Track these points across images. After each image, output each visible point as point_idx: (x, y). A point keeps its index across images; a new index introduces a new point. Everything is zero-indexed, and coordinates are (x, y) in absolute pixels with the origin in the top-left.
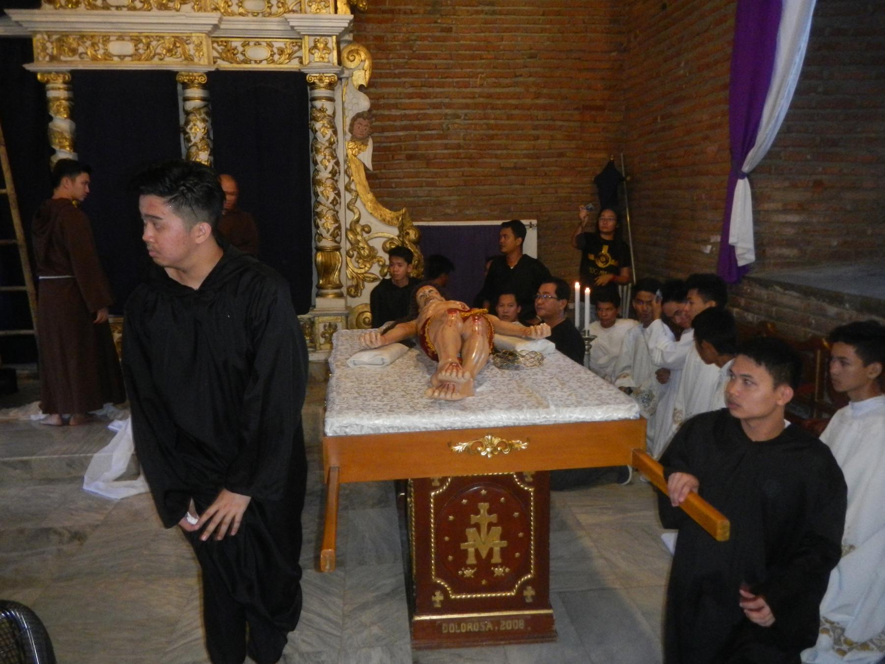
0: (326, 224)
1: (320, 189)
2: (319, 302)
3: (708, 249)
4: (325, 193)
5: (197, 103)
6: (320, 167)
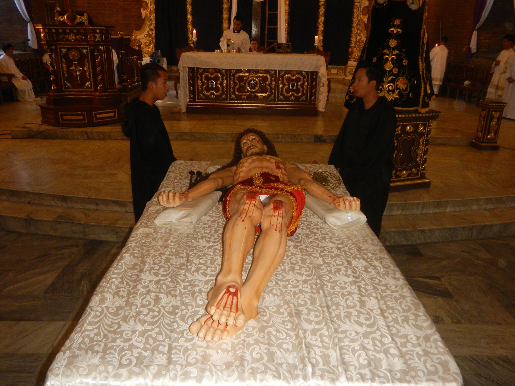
0: (353, 39)
1: (353, 29)
2: (349, 63)
3: (464, 49)
4: (354, 30)
5: (323, 3)
6: (354, 22)
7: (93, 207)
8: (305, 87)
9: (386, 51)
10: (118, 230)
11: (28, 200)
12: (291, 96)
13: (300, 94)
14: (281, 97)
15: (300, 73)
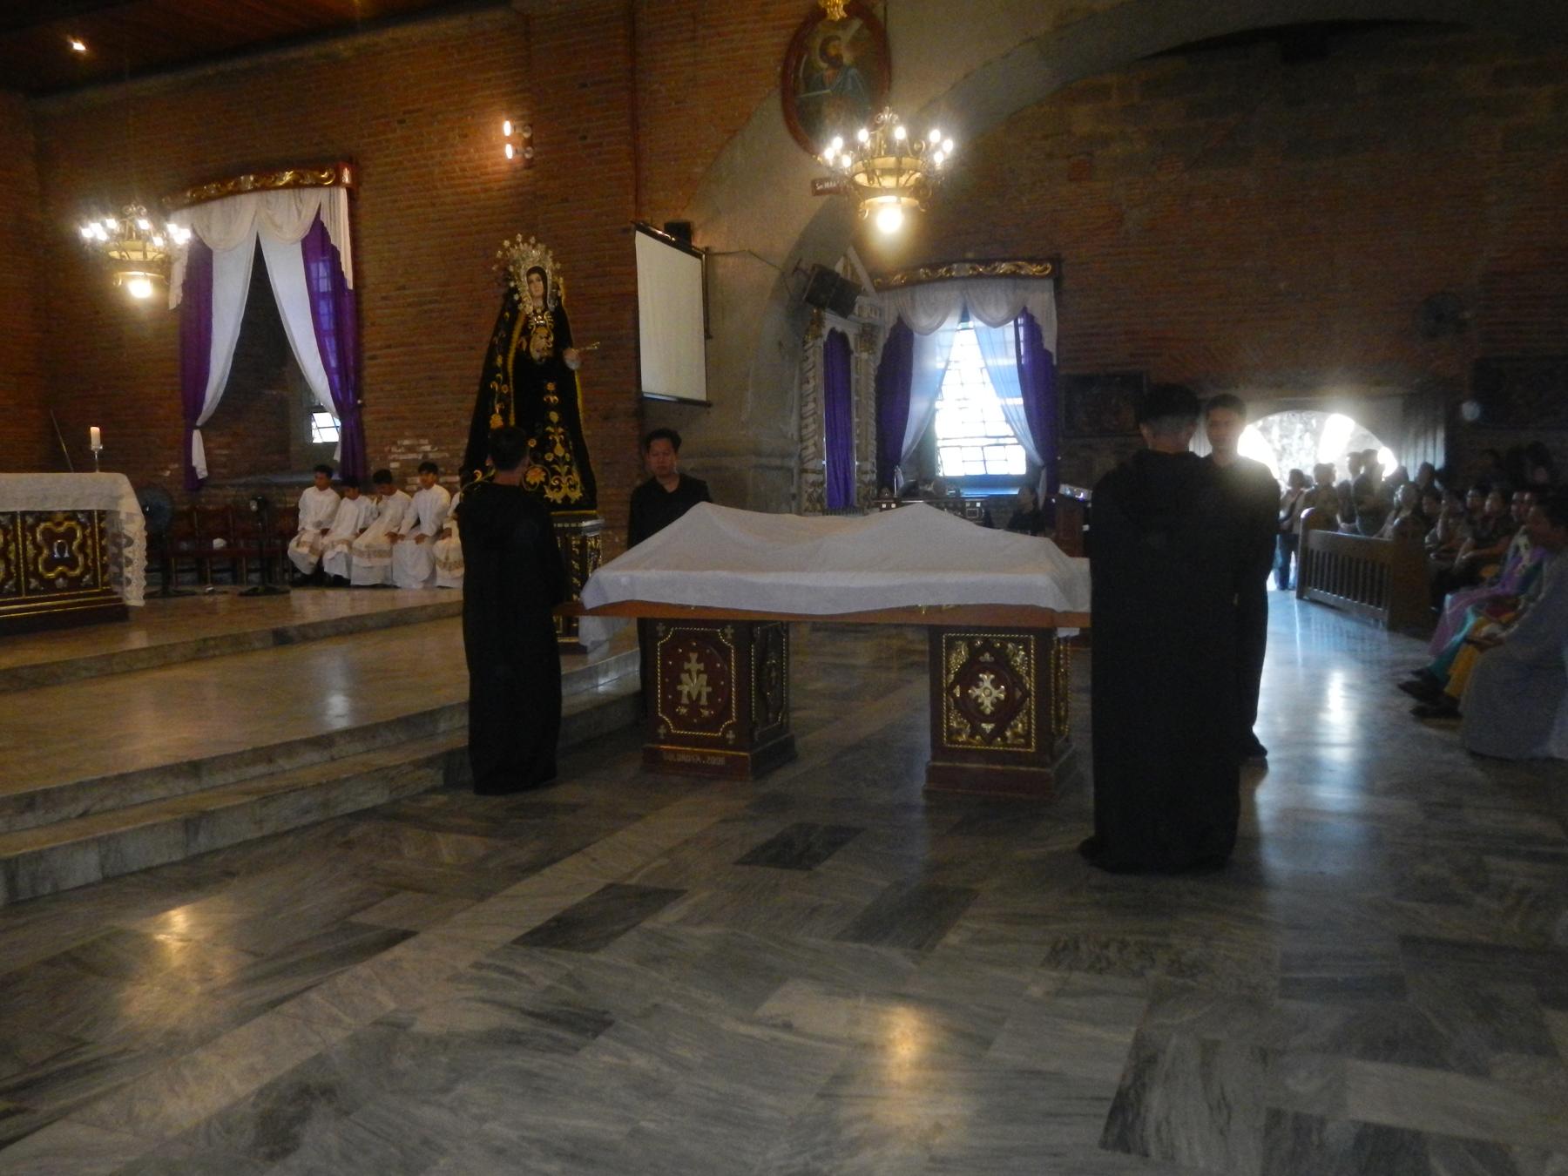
3: (168, 473)
7: (261, 769)
8: (89, 551)
9: (549, 429)
10: (393, 773)
11: (80, 808)
12: (58, 577)
13: (78, 572)
14: (34, 583)
15: (71, 516)
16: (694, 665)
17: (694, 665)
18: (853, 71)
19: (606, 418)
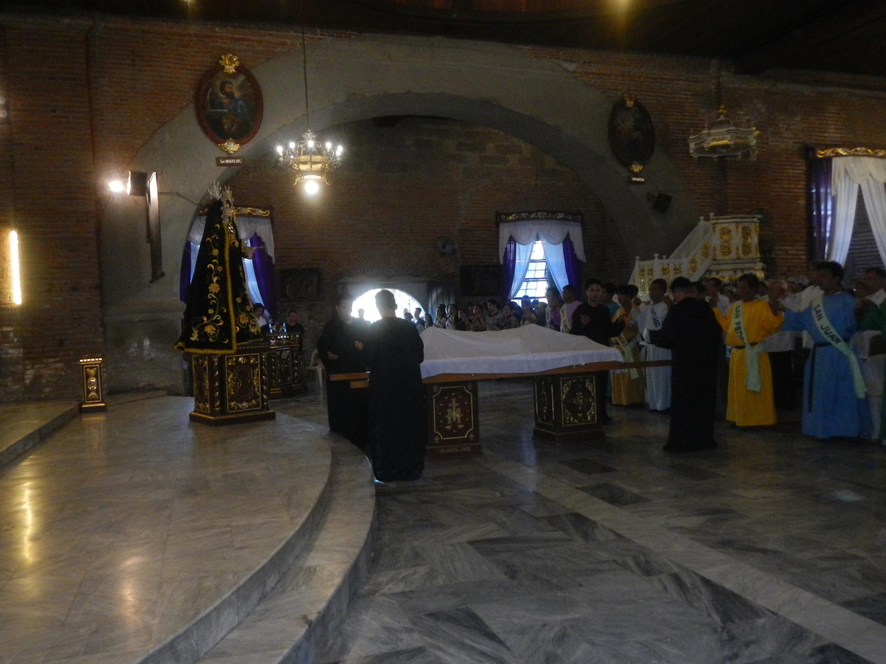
16: (454, 404)
17: (454, 404)
18: (240, 102)
19: (74, 289)
